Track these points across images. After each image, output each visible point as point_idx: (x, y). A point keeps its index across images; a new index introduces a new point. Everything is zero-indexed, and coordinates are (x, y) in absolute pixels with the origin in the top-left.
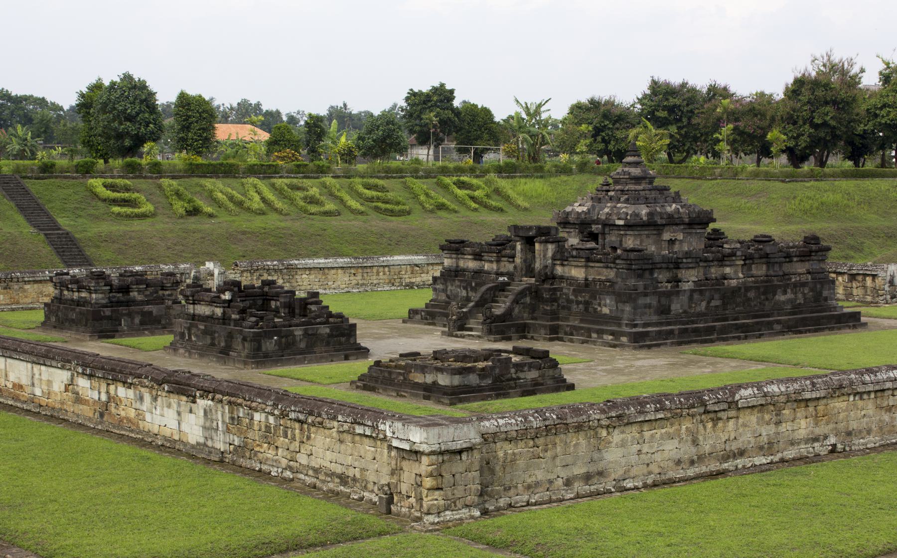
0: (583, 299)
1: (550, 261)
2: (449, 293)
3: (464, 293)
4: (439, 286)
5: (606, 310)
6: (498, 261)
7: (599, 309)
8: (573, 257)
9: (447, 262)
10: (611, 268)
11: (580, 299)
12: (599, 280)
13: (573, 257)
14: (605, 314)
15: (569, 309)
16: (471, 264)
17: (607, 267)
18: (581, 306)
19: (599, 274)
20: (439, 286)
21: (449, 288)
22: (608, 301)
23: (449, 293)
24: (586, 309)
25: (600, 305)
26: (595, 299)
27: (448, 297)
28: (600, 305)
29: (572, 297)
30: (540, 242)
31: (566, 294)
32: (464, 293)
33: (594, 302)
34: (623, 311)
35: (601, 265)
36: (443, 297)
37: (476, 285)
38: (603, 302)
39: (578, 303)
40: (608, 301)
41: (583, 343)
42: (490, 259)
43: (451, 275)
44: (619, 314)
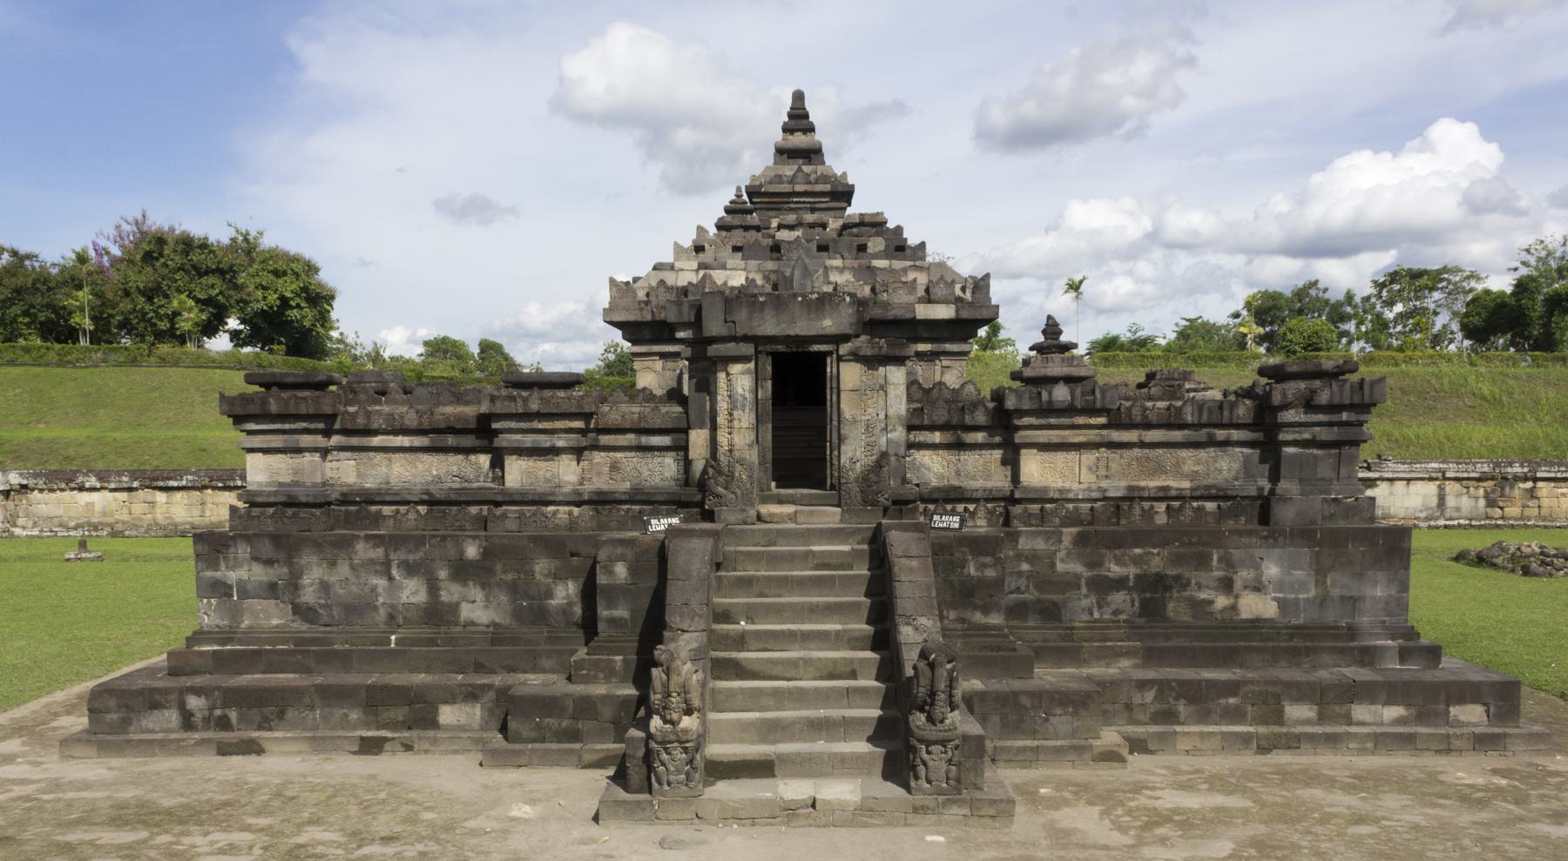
0: (1132, 571)
1: (899, 434)
2: (309, 596)
3: (412, 592)
4: (242, 571)
5: (1258, 606)
6: (578, 452)
7: (1222, 601)
8: (1049, 410)
9: (262, 471)
10: (1226, 443)
11: (1115, 570)
12: (1164, 495)
13: (1049, 410)
14: (1256, 623)
15: (1051, 613)
16: (408, 470)
17: (1212, 443)
18: (1119, 598)
19: (1159, 470)
20: (242, 571)
21: (314, 573)
22: (1272, 570)
23: (309, 596)
24: (1151, 610)
25: (1227, 585)
26: (1203, 562)
27: (300, 611)
28: (1227, 585)
29: (1068, 565)
30: (856, 357)
31: (1032, 557)
32: (412, 592)
33: (1195, 577)
34: (1352, 602)
35: (1177, 435)
36: (271, 617)
37: (487, 553)
38: (1243, 575)
39: (1103, 586)
40: (1272, 570)
41: (1263, 750)
42: (544, 441)
43: (286, 526)
44: (1331, 616)
